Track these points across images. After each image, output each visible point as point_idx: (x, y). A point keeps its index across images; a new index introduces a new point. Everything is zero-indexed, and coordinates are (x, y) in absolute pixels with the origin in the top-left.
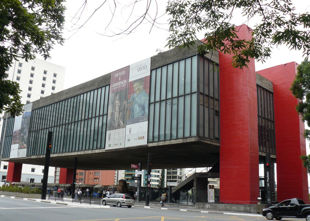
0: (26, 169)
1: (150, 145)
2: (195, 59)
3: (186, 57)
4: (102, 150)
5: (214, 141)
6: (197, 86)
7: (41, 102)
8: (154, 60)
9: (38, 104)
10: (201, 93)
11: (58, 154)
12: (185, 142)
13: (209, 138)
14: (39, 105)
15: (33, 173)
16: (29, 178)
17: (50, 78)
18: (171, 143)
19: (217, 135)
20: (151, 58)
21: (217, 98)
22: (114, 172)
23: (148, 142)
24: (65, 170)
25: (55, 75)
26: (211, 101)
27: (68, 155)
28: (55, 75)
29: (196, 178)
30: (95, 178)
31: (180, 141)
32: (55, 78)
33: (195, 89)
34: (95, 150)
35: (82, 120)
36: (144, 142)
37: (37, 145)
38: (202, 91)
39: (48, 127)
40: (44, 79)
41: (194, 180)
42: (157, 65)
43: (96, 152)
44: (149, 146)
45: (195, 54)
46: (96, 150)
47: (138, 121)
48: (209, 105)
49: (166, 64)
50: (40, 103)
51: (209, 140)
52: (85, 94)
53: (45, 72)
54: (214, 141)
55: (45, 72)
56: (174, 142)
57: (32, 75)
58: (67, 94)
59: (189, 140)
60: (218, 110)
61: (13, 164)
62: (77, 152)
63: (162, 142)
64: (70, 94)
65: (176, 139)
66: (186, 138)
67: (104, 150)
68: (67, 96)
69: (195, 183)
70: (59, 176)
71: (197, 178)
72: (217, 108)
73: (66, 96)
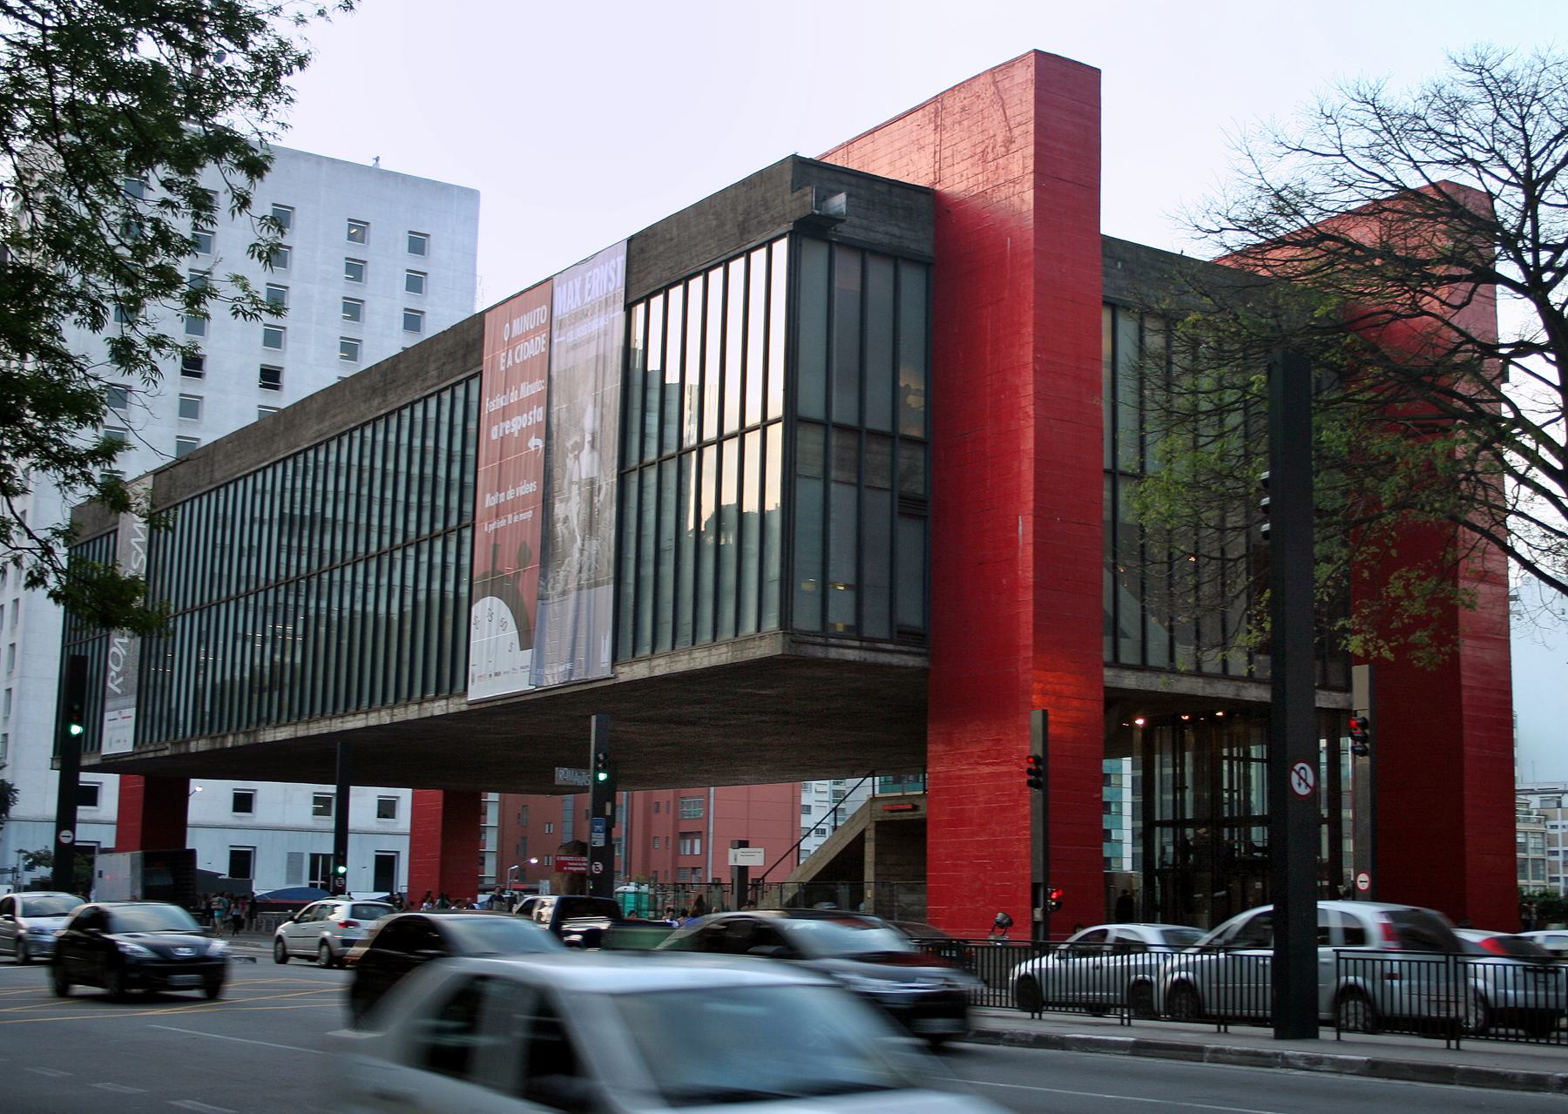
2: (781, 248)
3: (749, 246)
4: (457, 700)
5: (890, 647)
6: (786, 390)
7: (221, 457)
8: (640, 248)
9: (208, 469)
11: (292, 729)
13: (856, 631)
14: (212, 471)
16: (301, 855)
19: (911, 613)
20: (630, 240)
21: (916, 432)
22: (796, 798)
24: (435, 797)
26: (877, 454)
27: (333, 729)
29: (872, 826)
30: (684, 835)
31: (720, 656)
34: (432, 700)
35: (395, 546)
37: (167, 692)
39: (399, 540)
41: (867, 835)
42: (651, 281)
43: (437, 712)
44: (623, 678)
45: (780, 231)
46: (436, 704)
48: (859, 478)
49: (679, 277)
50: (217, 465)
51: (857, 644)
52: (471, 382)
54: (890, 647)
56: (703, 659)
58: (322, 421)
60: (920, 491)
61: (138, 782)
62: (364, 716)
63: (662, 661)
64: (334, 416)
65: (709, 648)
66: (751, 639)
67: (463, 701)
68: (321, 426)
70: (333, 835)
71: (877, 822)
72: (916, 486)
73: (316, 428)
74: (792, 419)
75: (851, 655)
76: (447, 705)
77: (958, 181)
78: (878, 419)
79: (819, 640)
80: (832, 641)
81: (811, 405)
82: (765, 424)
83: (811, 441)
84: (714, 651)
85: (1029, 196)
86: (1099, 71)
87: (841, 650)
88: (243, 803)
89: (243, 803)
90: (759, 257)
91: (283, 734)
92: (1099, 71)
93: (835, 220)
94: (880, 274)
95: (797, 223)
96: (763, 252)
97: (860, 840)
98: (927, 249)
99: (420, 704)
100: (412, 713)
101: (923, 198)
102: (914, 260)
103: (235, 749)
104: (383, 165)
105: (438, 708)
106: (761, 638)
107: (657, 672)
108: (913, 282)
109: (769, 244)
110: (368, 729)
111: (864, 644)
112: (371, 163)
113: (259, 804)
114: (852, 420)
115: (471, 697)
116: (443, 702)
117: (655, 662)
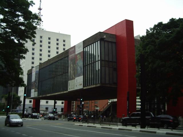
0: (43, 102)
1: (85, 88)
2: (99, 42)
8: (84, 42)
10: (102, 60)
12: (96, 86)
15: (47, 104)
17: (61, 43)
20: (83, 41)
23: (83, 87)
25: (64, 41)
28: (64, 41)
32: (64, 43)
36: (81, 87)
38: (103, 59)
40: (57, 44)
42: (85, 45)
44: (84, 89)
47: (79, 76)
53: (58, 40)
55: (58, 40)
56: (92, 86)
57: (49, 43)
65: (93, 85)
69: (111, 107)
74: (101, 60)
75: (108, 86)
77: (118, 34)
78: (111, 60)
81: (103, 59)
83: (103, 62)
85: (126, 35)
86: (132, 22)
88: (47, 102)
89: (47, 102)
90: (97, 43)
91: (49, 95)
92: (133, 21)
93: (105, 38)
94: (110, 44)
95: (100, 39)
97: (110, 107)
98: (115, 41)
100: (62, 93)
101: (114, 36)
102: (114, 42)
103: (44, 97)
104: (60, 33)
105: (65, 92)
107: (88, 88)
108: (114, 45)
109: (98, 41)
110: (58, 94)
112: (58, 32)
113: (49, 102)
114: (108, 60)
115: (68, 91)
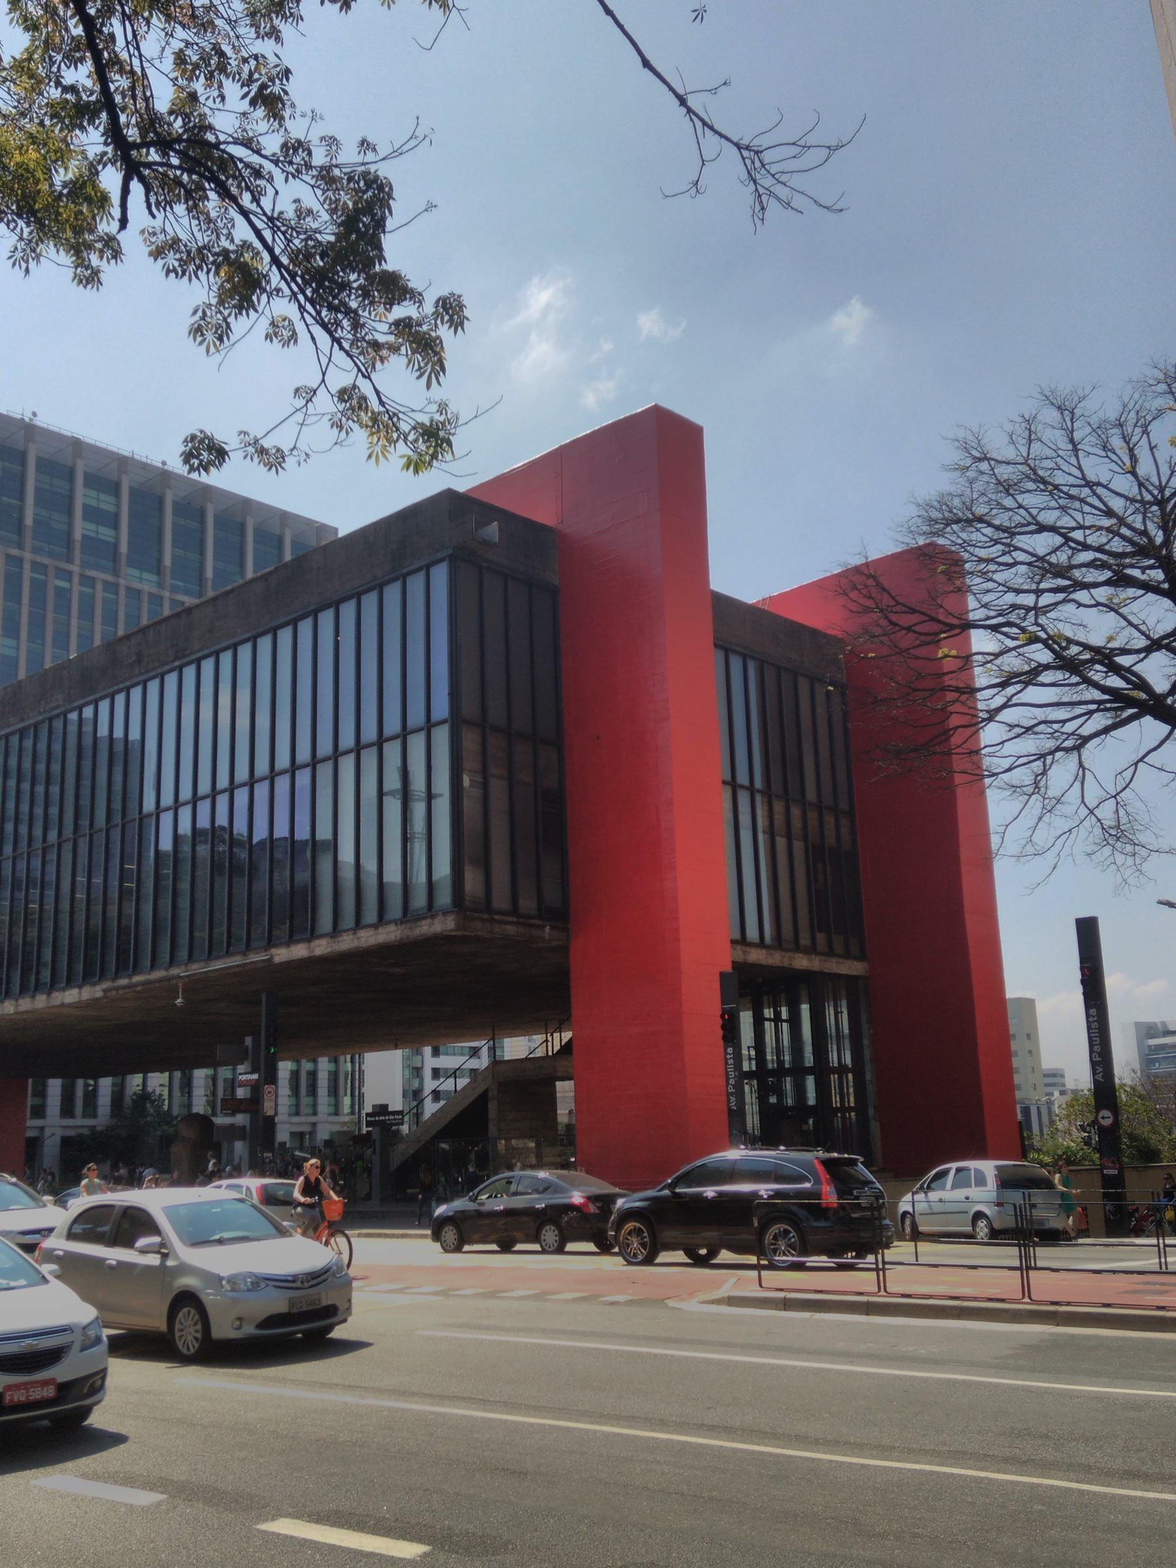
18: (355, 944)
33: (441, 707)
34: (64, 990)
46: (67, 993)
51: (515, 919)
56: (368, 938)
59: (427, 928)
65: (375, 926)
74: (456, 721)
75: (511, 930)
76: (80, 993)
79: (486, 916)
80: (497, 917)
81: (470, 708)
82: (429, 726)
83: (470, 741)
84: (381, 930)
87: (504, 926)
96: (420, 577)
99: (49, 994)
106: (433, 917)
107: (318, 952)
111: (521, 920)
116: (75, 991)
117: (316, 943)
